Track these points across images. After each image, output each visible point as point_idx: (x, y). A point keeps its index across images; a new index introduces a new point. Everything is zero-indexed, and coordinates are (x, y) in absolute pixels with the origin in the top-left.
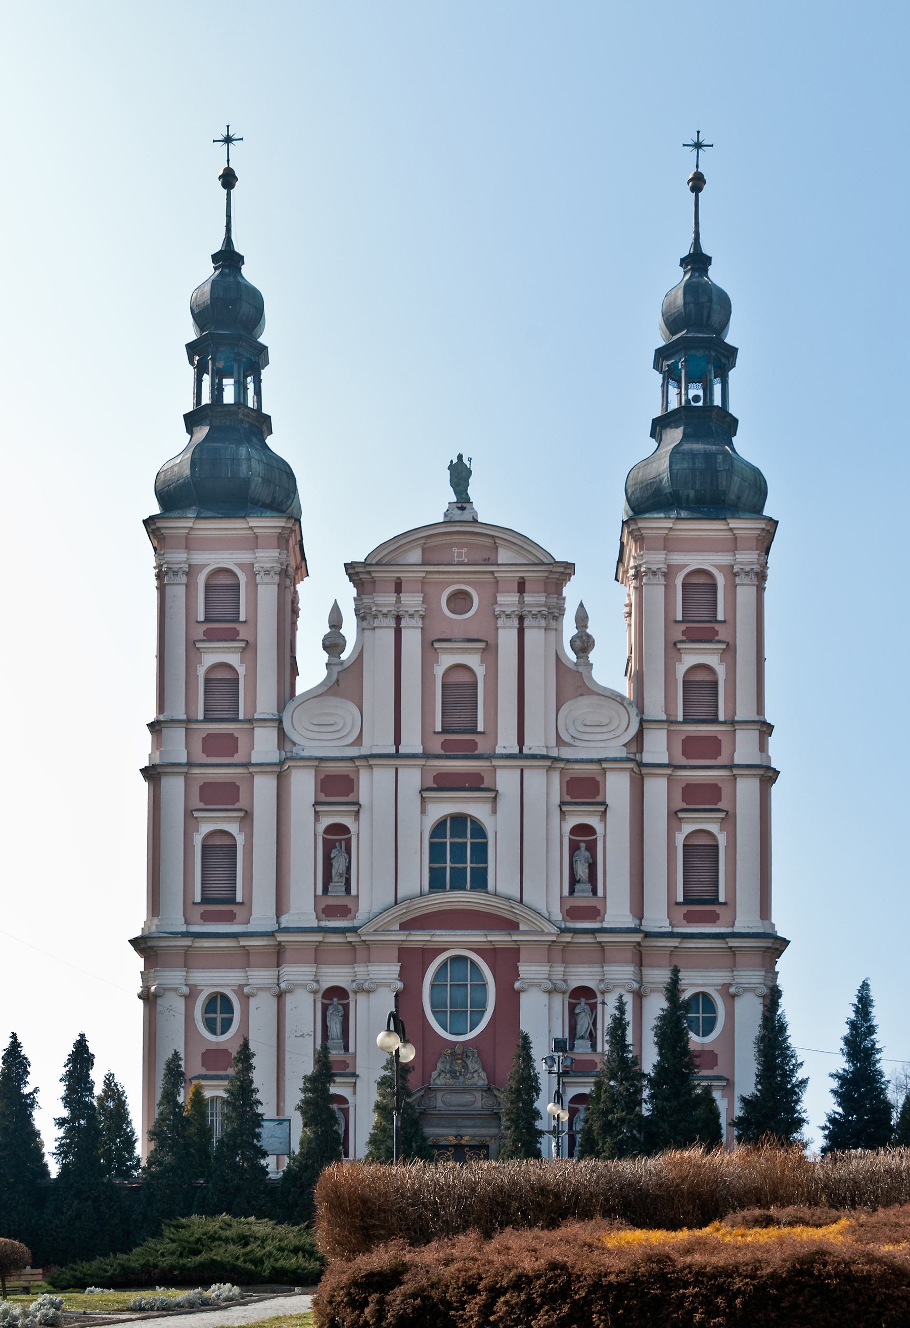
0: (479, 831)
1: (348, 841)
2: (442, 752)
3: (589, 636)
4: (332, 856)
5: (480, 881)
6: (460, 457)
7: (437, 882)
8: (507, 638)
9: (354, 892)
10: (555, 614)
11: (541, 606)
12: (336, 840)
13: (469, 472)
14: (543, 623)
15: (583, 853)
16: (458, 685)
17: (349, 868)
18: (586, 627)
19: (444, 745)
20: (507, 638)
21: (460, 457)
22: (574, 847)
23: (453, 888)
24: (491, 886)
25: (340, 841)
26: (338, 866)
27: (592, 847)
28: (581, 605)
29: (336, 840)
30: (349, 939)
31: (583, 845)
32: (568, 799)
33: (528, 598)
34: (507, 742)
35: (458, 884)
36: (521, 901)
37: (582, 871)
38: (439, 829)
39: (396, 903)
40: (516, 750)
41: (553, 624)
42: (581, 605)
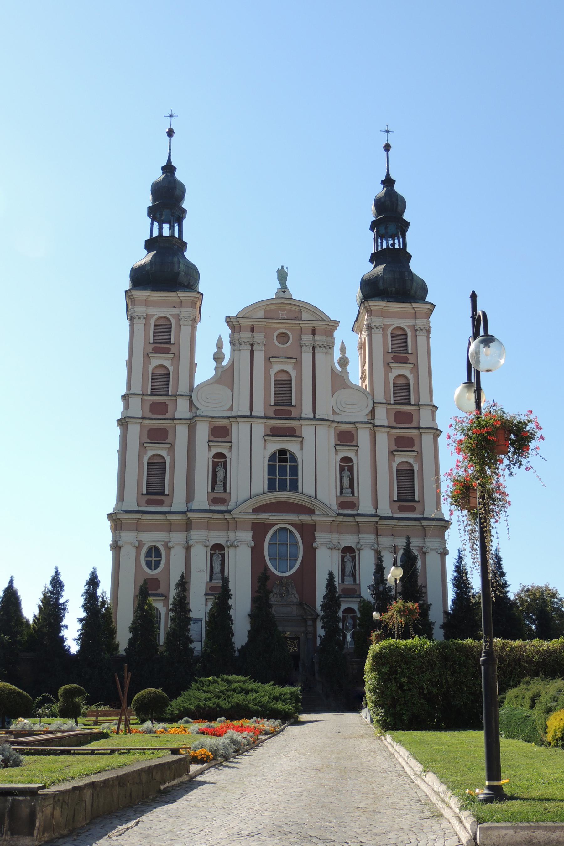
0: (294, 459)
1: (225, 463)
2: (274, 416)
3: (347, 358)
4: (217, 470)
5: (294, 487)
6: (282, 267)
7: (271, 487)
8: (307, 357)
9: (228, 491)
10: (330, 346)
11: (324, 342)
12: (219, 462)
13: (287, 274)
14: (325, 350)
15: (347, 473)
16: (282, 381)
17: (225, 477)
18: (345, 353)
19: (275, 412)
20: (307, 357)
21: (282, 267)
22: (342, 469)
23: (280, 490)
24: (300, 489)
25: (221, 462)
26: (220, 476)
27: (351, 469)
28: (343, 342)
29: (219, 462)
30: (226, 517)
31: (346, 468)
32: (339, 443)
33: (317, 337)
34: (307, 412)
35: (282, 488)
36: (316, 498)
37: (346, 482)
38: (272, 458)
39: (251, 498)
40: (312, 416)
41: (329, 351)
42: (343, 342)
